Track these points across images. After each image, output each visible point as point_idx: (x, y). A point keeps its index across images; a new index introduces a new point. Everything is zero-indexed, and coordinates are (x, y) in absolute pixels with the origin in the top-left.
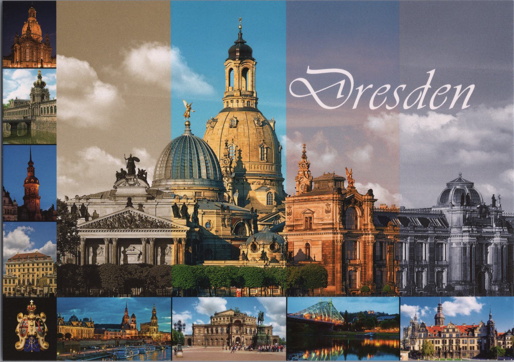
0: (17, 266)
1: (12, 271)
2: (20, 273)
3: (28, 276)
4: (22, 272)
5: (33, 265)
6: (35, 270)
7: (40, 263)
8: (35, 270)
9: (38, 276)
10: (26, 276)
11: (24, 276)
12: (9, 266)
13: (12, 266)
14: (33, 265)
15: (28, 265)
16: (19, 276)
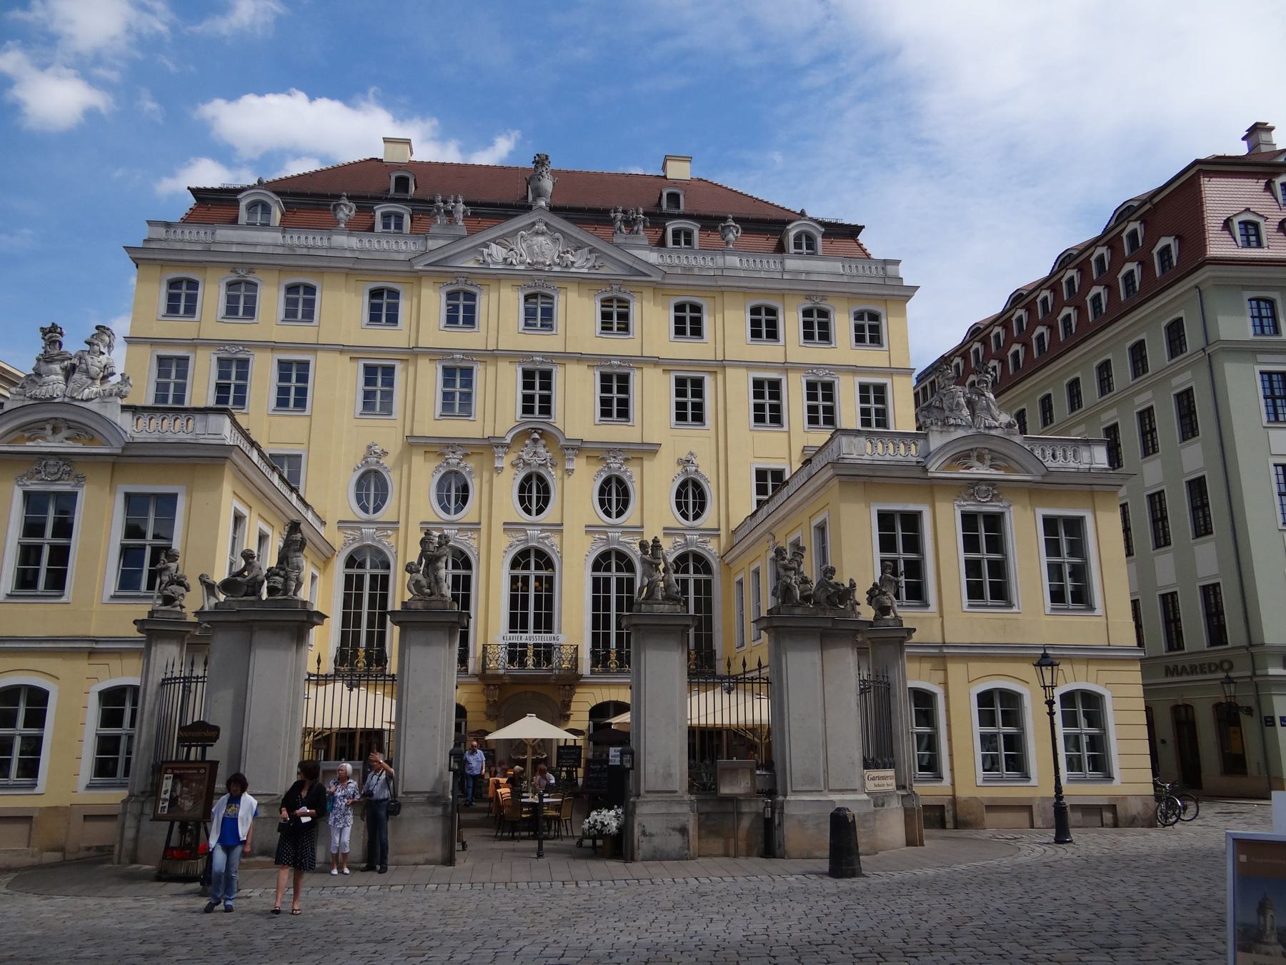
0: (342, 310)
1: (230, 394)
2: (386, 434)
3: (535, 492)
4: (431, 423)
5: (615, 318)
6: (653, 395)
7: (722, 288)
8: (653, 395)
9: (691, 496)
10: (498, 494)
11: (455, 492)
12: (181, 298)
13: (241, 303)
14: (615, 318)
15: (540, 312)
16: (372, 487)
